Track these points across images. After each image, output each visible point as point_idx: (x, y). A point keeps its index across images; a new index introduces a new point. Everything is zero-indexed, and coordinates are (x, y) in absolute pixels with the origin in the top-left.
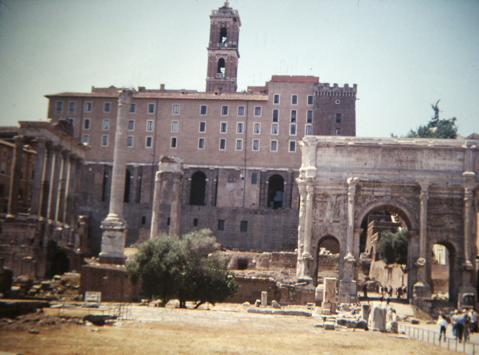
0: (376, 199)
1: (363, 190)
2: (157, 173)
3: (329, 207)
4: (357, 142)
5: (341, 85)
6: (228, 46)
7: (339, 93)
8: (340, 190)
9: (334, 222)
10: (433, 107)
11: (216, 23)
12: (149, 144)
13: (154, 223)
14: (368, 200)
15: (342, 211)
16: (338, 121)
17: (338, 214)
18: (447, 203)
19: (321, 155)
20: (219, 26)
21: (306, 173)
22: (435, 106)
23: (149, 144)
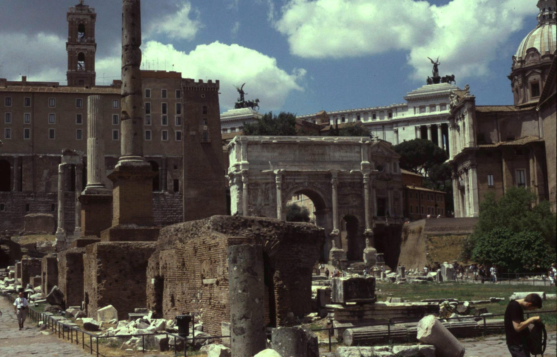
0: (297, 185)
1: (287, 179)
2: (60, 165)
3: (259, 193)
4: (279, 140)
5: (205, 81)
6: (87, 42)
7: (204, 88)
8: (269, 179)
9: (265, 205)
10: (239, 90)
11: (74, 20)
12: (27, 136)
13: (61, 211)
14: (291, 187)
15: (271, 195)
16: (205, 112)
17: (268, 199)
18: (350, 186)
19: (251, 152)
20: (77, 22)
21: (241, 166)
22: (240, 89)
23: (27, 136)
